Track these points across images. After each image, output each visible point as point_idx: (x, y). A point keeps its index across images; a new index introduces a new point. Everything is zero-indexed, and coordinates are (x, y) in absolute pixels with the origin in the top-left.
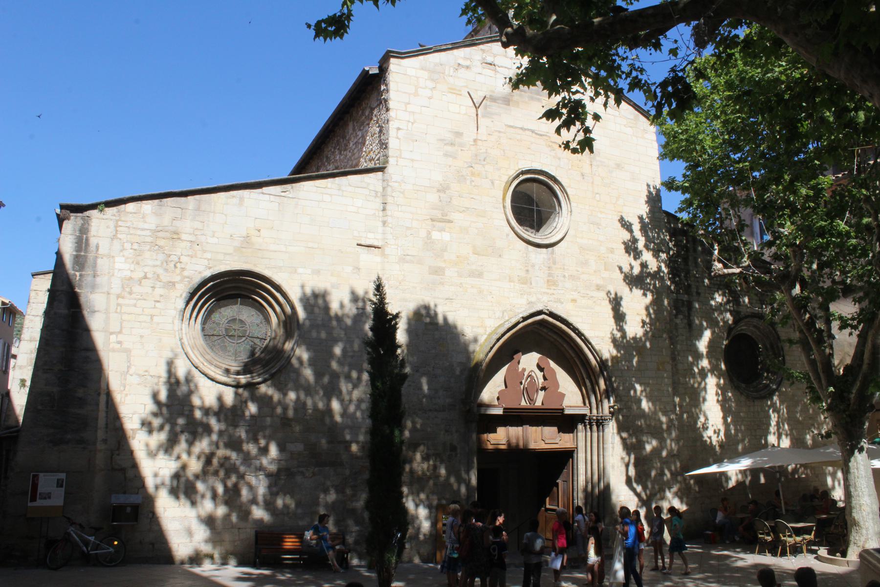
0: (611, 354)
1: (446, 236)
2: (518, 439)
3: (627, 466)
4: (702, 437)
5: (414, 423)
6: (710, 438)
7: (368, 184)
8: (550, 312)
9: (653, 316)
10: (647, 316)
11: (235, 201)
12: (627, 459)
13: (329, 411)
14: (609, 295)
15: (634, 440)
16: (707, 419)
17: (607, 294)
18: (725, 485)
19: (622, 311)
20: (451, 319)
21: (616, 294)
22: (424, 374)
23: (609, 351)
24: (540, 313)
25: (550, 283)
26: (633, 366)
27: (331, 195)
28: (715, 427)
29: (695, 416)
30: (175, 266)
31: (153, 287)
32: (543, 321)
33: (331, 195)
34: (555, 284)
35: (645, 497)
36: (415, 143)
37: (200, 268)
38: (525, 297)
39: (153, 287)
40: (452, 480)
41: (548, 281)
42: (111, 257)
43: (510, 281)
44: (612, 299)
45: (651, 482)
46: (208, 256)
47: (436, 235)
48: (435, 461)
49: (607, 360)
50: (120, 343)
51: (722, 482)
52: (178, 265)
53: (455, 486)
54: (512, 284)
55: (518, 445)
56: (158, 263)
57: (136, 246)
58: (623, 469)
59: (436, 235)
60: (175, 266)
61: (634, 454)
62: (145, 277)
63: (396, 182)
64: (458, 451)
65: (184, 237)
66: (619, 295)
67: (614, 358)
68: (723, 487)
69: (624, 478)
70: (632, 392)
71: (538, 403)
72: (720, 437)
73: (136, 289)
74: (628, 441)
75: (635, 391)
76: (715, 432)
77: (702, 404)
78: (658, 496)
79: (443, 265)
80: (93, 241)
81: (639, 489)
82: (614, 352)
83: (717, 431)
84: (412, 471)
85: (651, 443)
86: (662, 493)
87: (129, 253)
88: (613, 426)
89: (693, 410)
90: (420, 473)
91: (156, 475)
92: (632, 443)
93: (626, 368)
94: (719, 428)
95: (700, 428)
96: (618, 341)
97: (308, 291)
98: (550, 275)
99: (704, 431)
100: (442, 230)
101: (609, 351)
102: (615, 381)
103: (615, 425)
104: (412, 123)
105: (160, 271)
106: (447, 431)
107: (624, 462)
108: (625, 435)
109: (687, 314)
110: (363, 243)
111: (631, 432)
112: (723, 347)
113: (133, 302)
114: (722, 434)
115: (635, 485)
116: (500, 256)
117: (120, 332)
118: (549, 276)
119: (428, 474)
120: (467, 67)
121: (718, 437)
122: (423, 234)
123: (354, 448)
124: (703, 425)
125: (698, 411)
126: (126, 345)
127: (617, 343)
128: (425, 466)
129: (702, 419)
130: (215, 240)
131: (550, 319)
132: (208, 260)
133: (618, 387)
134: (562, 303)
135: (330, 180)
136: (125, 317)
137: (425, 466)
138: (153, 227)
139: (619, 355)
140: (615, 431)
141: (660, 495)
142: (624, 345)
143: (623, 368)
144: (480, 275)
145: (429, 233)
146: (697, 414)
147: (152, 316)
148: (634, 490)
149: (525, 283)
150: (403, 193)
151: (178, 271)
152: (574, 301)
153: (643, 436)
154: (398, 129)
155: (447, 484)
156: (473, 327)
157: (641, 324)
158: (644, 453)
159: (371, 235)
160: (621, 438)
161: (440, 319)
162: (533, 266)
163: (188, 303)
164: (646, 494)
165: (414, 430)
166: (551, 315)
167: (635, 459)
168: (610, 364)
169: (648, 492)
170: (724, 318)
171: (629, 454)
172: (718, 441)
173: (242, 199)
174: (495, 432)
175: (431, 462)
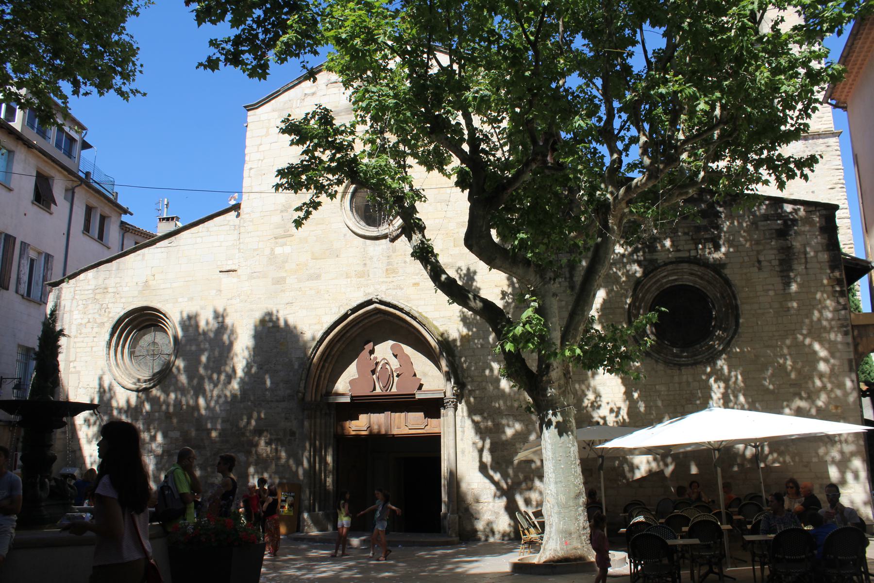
0: (460, 333)
1: (287, 249)
2: (379, 426)
3: (481, 451)
4: (592, 418)
5: (259, 413)
6: (604, 418)
7: (229, 221)
8: (380, 301)
9: (517, 285)
10: (509, 286)
11: (140, 258)
12: (480, 444)
13: (197, 407)
14: (459, 271)
15: (490, 423)
16: (598, 395)
17: (457, 271)
18: (629, 475)
19: (476, 287)
20: (291, 322)
21: (468, 269)
22: (267, 372)
23: (458, 331)
24: (370, 302)
25: (389, 272)
26: (489, 343)
27: (202, 237)
28: (612, 405)
29: (579, 393)
30: (105, 311)
31: (92, 328)
32: (376, 309)
33: (202, 237)
34: (394, 271)
35: (505, 486)
36: (263, 177)
37: (119, 310)
38: (362, 289)
39: (92, 328)
40: (291, 462)
41: (387, 270)
42: (71, 311)
43: (348, 276)
44: (463, 276)
45: (513, 469)
46: (123, 300)
47: (278, 250)
48: (277, 445)
49: (455, 340)
50: (75, 367)
51: (624, 470)
52: (107, 310)
53: (294, 468)
54: (349, 279)
55: (379, 432)
56: (96, 311)
57: (84, 303)
58: (476, 455)
59: (278, 250)
60: (105, 311)
61: (490, 438)
62: (89, 322)
63: (247, 214)
64: (297, 435)
65: (110, 290)
66: (472, 269)
67: (463, 338)
68: (625, 477)
69: (477, 464)
70: (487, 372)
71: (394, 390)
72: (620, 417)
73: (84, 330)
74: (482, 425)
75: (492, 370)
76: (612, 411)
77: (591, 379)
78: (524, 486)
79: (284, 275)
80: (63, 303)
81: (497, 477)
82: (465, 331)
83: (616, 410)
84: (258, 454)
85: (513, 426)
86: (529, 483)
87: (81, 307)
88: (462, 409)
89: (577, 386)
90: (264, 455)
91: (91, 456)
92: (486, 428)
93: (479, 346)
94: (618, 405)
95: (587, 406)
96: (469, 319)
97: (185, 316)
98: (389, 264)
99: (594, 410)
100: (282, 246)
101: (458, 331)
102: (465, 361)
103: (465, 408)
104: (262, 160)
105: (97, 316)
106: (286, 419)
107: (476, 447)
108: (477, 418)
109: (568, 275)
110: (224, 269)
111: (485, 415)
112: (627, 306)
113: (82, 339)
114: (624, 413)
115: (491, 473)
116: (337, 256)
117: (75, 360)
118: (388, 265)
119: (271, 456)
120: (313, 94)
121: (617, 416)
122: (267, 252)
123: (214, 434)
124: (592, 403)
125: (583, 387)
126: (78, 369)
127: (468, 321)
128: (269, 449)
129: (591, 396)
130: (127, 289)
131: (383, 307)
132: (124, 303)
133: (469, 368)
134: (402, 289)
135: (201, 226)
136: (78, 350)
137: (269, 449)
138: (93, 287)
139: (470, 333)
140: (465, 414)
141: (527, 484)
142: (477, 322)
143: (475, 347)
144: (318, 277)
145: (272, 250)
146: (583, 391)
147: (92, 347)
148: (491, 479)
149: (363, 277)
150: (252, 221)
151: (106, 314)
152: (416, 284)
153: (502, 418)
154: (251, 169)
155: (287, 466)
156: (310, 325)
157: (501, 296)
158: (504, 438)
159: (230, 262)
160: (473, 421)
161: (282, 323)
162: (371, 258)
163: (112, 335)
164: (507, 483)
165: (259, 419)
166: (381, 302)
167: (492, 444)
168: (458, 344)
169: (509, 481)
170: (628, 271)
171: (484, 440)
172: (617, 422)
173: (144, 255)
174: (358, 419)
175: (273, 446)
